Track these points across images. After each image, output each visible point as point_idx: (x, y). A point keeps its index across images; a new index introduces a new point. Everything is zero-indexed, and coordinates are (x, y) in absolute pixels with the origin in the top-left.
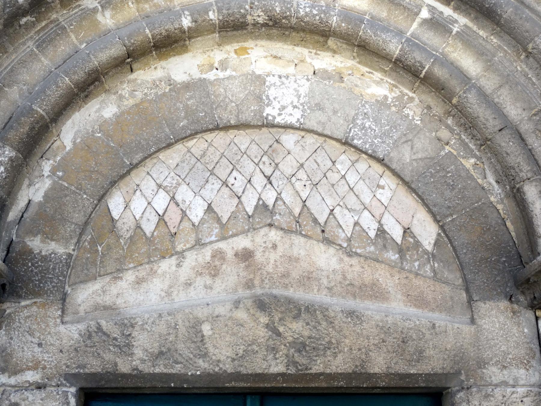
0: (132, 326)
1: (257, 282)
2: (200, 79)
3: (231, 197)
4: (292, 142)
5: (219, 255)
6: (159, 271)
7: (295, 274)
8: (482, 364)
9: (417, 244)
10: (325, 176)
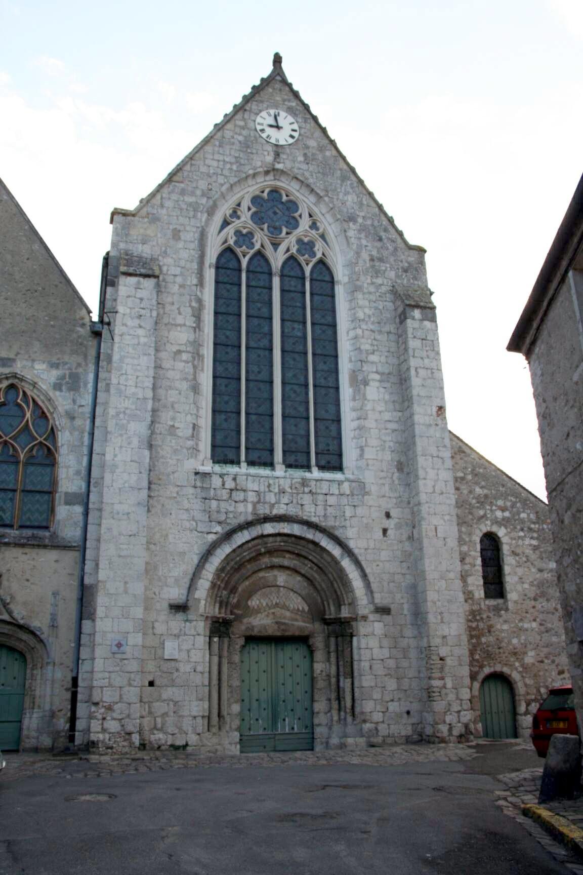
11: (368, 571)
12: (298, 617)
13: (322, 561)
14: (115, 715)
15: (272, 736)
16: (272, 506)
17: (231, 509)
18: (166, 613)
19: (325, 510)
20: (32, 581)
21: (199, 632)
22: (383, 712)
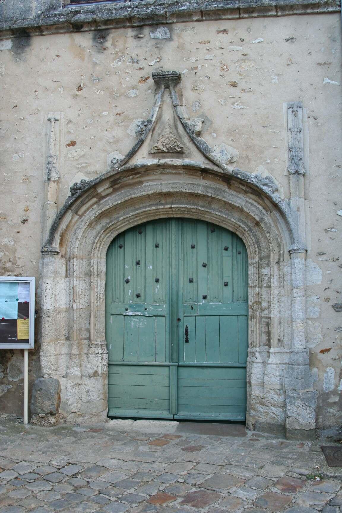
20: (242, 85)
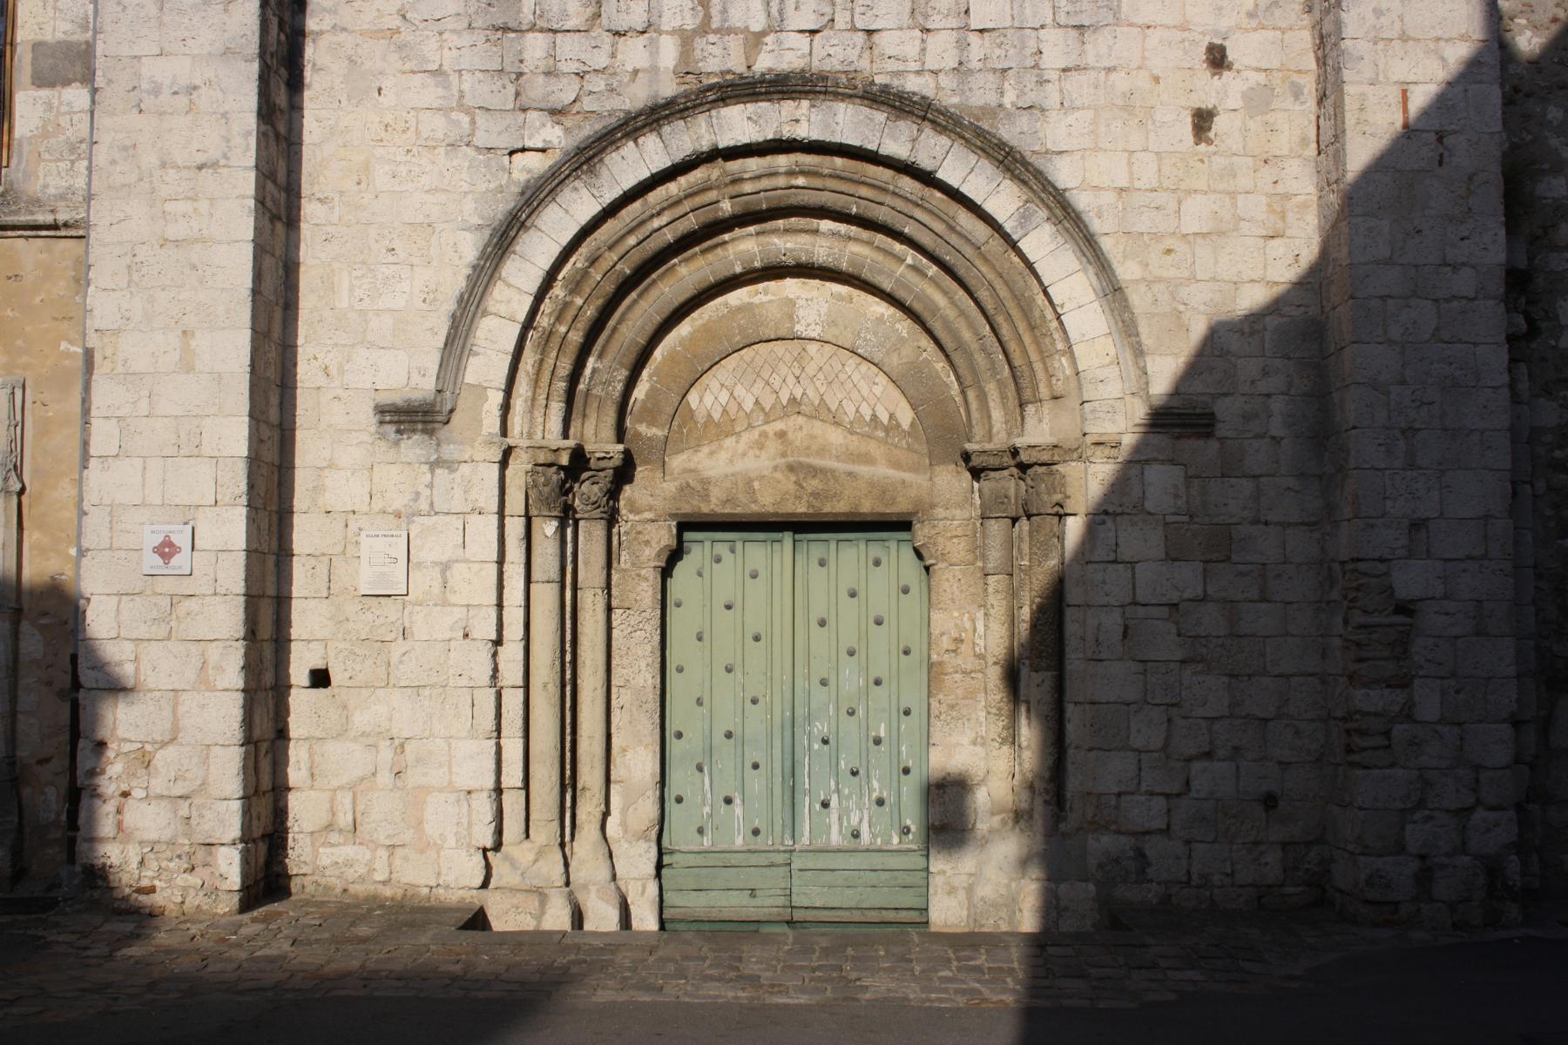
0: (709, 483)
1: (789, 452)
2: (748, 303)
3: (772, 393)
4: (814, 350)
5: (764, 434)
6: (725, 446)
7: (814, 447)
8: (933, 506)
9: (898, 425)
10: (837, 376)
11: (1126, 271)
12: (874, 449)
13: (954, 239)
14: (158, 785)
15: (780, 859)
16: (755, 40)
17: (600, 60)
18: (365, 437)
19: (963, 45)
21: (481, 504)
22: (1167, 796)
